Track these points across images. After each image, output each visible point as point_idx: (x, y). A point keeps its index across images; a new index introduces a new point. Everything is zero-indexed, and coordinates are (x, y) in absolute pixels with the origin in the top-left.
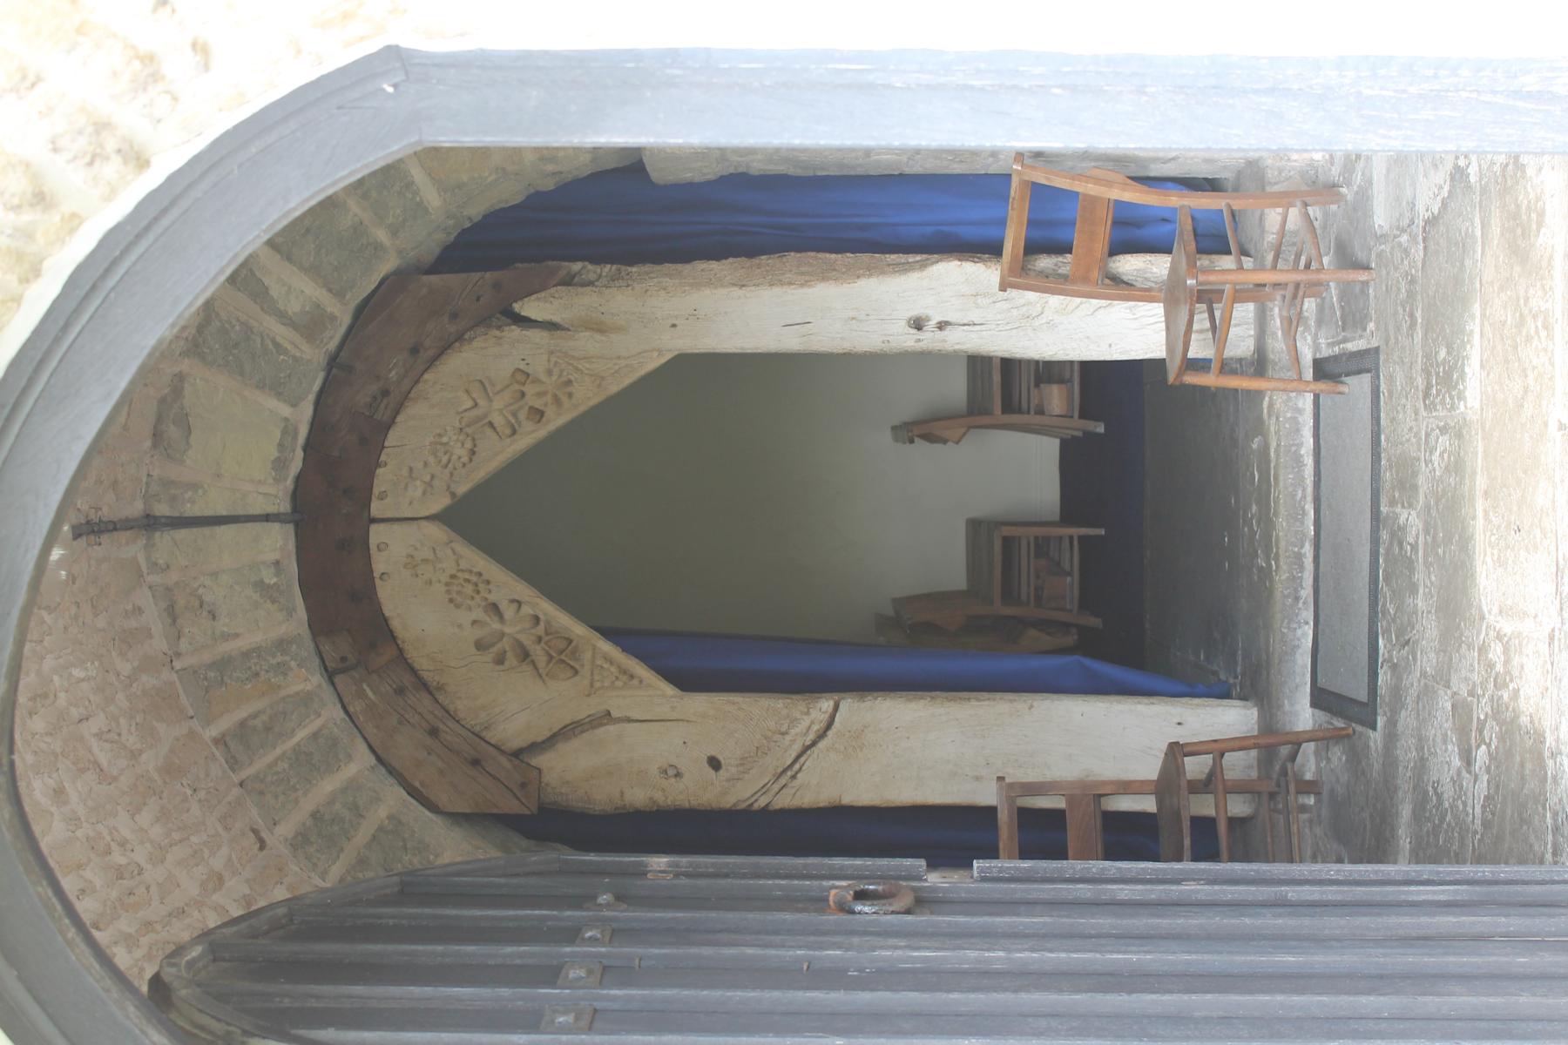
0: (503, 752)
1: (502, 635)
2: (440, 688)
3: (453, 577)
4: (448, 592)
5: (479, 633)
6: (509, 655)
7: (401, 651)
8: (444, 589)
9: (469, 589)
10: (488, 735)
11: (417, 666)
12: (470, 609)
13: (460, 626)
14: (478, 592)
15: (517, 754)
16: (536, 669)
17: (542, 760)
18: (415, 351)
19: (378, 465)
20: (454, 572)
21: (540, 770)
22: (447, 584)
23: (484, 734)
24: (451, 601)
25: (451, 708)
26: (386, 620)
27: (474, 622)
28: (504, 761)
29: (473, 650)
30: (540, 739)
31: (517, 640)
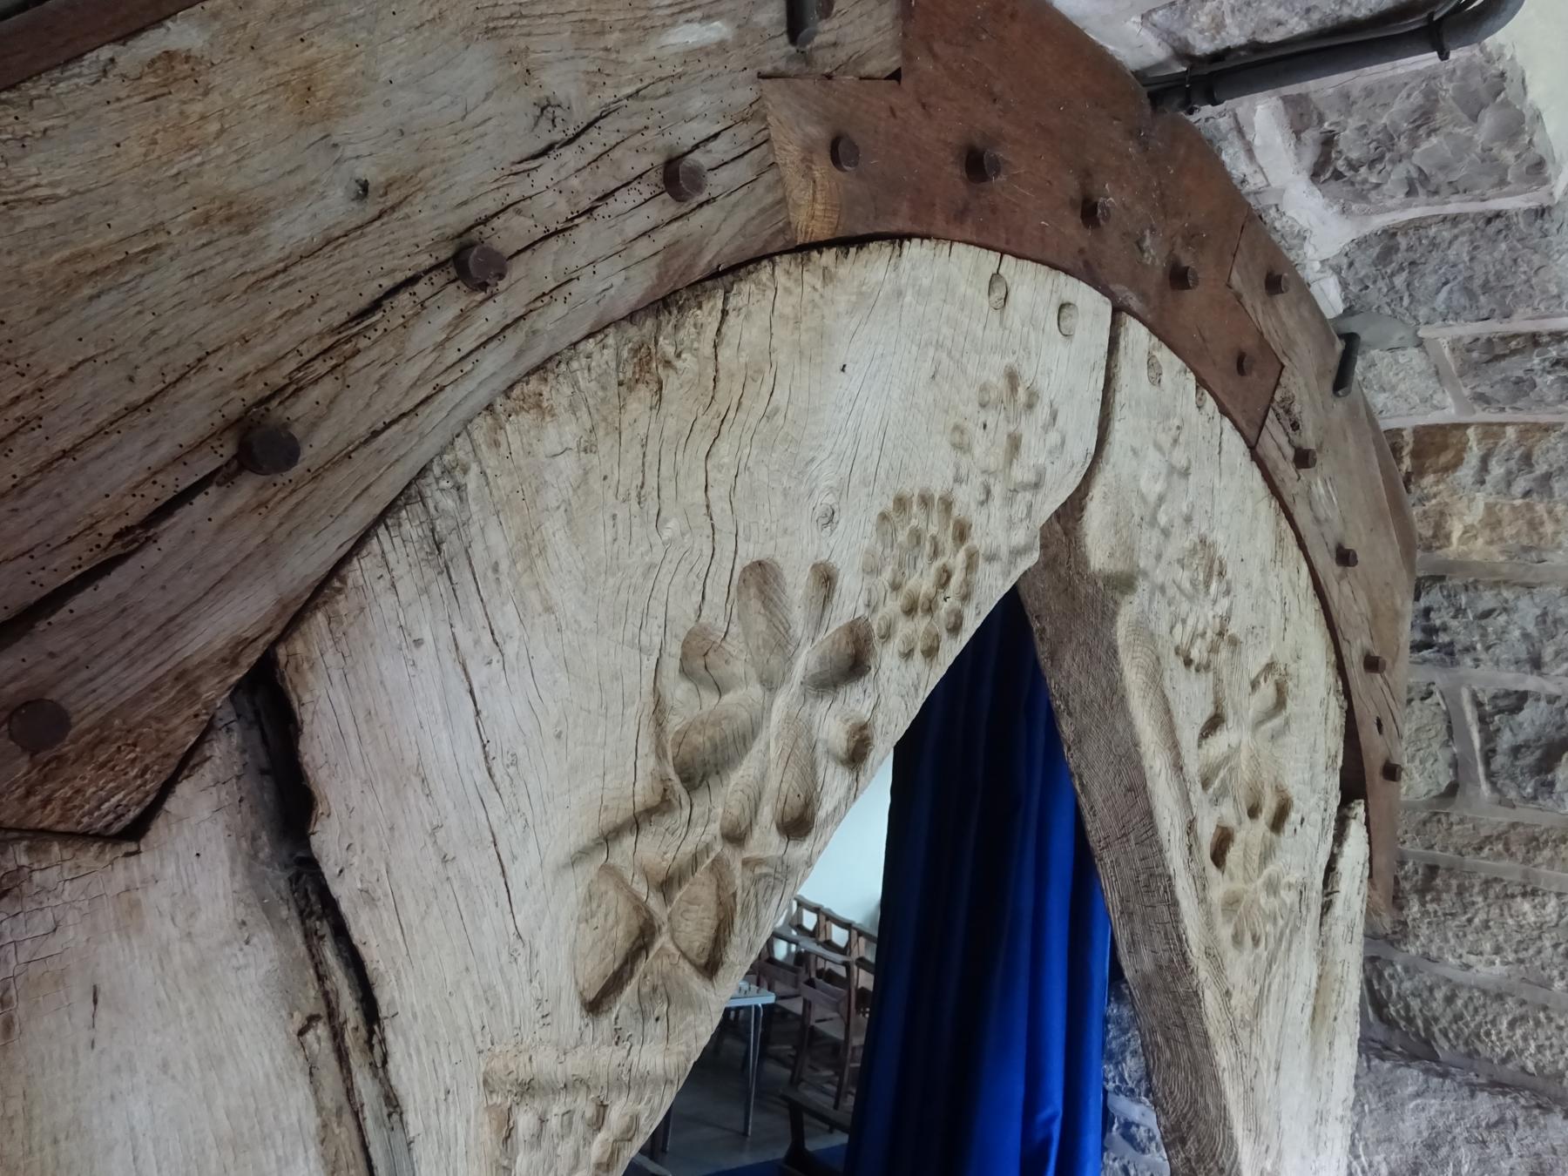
0: (295, 618)
1: (770, 685)
2: (645, 368)
3: (962, 533)
4: (925, 501)
5: (797, 586)
6: (710, 700)
7: (804, 249)
8: (937, 491)
9: (922, 582)
10: (398, 549)
11: (746, 292)
12: (872, 570)
13: (830, 518)
14: (910, 611)
15: (267, 703)
16: (637, 822)
17: (204, 836)
18: (1345, 557)
19: (1201, 383)
20: (977, 540)
21: (134, 832)
22: (947, 504)
23: (410, 525)
24: (901, 503)
25: (557, 393)
26: (898, 238)
27: (826, 579)
28: (242, 613)
29: (750, 552)
30: (327, 841)
31: (744, 739)
